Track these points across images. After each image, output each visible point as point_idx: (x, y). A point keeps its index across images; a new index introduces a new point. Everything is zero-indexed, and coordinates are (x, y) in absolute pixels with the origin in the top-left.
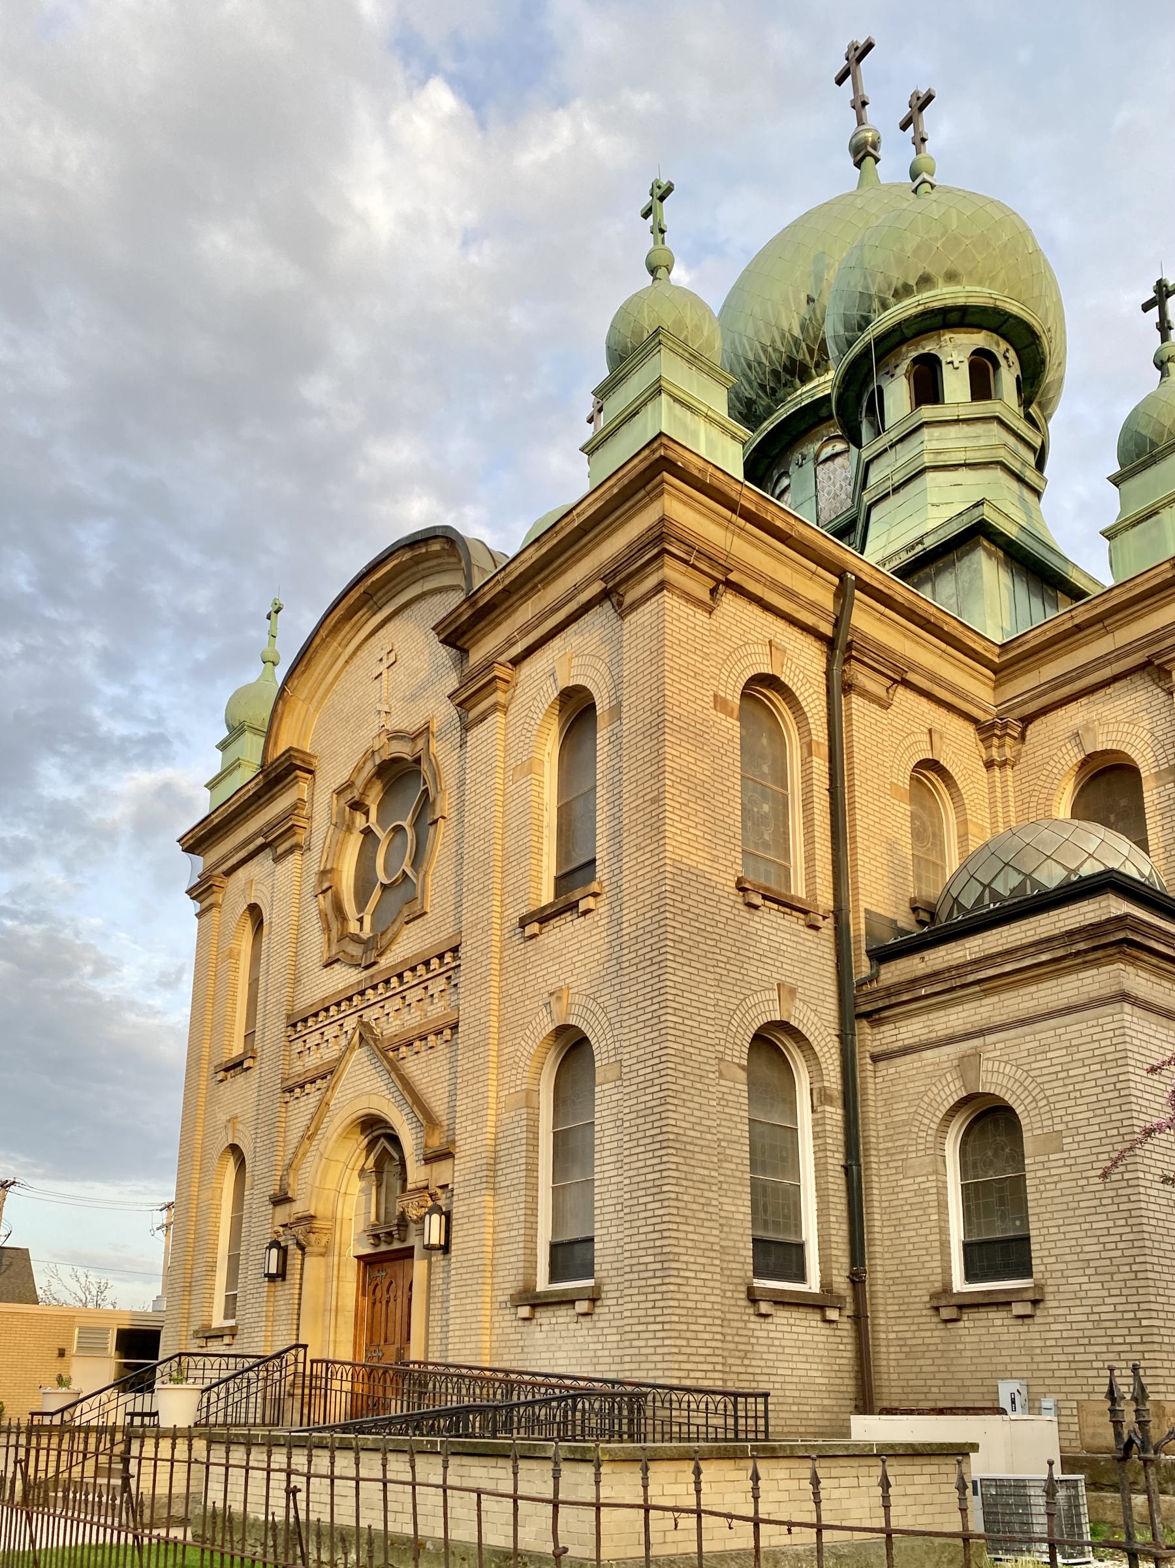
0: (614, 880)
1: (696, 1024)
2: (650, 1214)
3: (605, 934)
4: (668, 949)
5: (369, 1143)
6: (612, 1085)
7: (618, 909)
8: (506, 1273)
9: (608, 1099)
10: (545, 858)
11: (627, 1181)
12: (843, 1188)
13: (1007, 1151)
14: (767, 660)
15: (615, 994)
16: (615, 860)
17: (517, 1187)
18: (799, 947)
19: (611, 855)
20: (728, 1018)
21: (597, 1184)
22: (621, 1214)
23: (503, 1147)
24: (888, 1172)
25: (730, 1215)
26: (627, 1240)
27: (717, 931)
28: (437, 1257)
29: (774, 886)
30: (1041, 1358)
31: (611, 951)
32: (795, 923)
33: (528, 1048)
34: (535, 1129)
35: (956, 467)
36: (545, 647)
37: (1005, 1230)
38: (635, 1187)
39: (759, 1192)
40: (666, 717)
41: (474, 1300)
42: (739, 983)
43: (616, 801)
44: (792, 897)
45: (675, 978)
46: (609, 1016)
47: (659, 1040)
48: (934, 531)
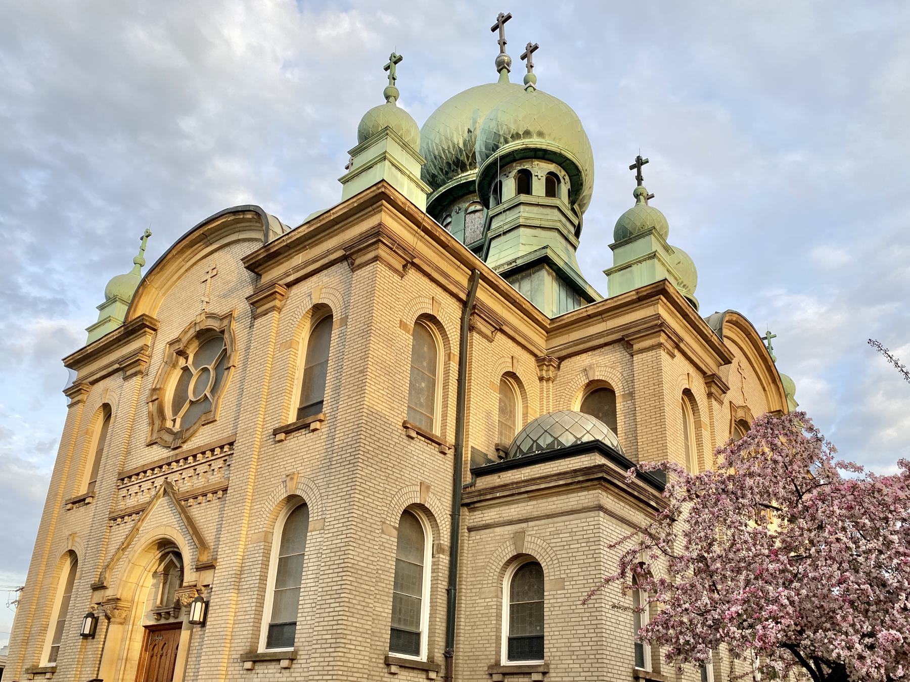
0: (333, 413)
1: (371, 501)
3: (324, 444)
4: (360, 456)
5: (162, 556)
6: (318, 532)
7: (333, 430)
9: (314, 541)
10: (293, 397)
11: (320, 590)
13: (536, 587)
14: (430, 306)
15: (325, 479)
17: (253, 589)
18: (434, 463)
20: (390, 499)
21: (302, 590)
23: (247, 564)
25: (379, 614)
27: (389, 449)
29: (423, 428)
32: (433, 449)
33: (269, 506)
34: (268, 556)
36: (307, 280)
37: (530, 632)
38: (325, 593)
43: (339, 369)
44: (433, 435)
45: (362, 473)
46: (321, 491)
47: (349, 508)
48: (522, 257)
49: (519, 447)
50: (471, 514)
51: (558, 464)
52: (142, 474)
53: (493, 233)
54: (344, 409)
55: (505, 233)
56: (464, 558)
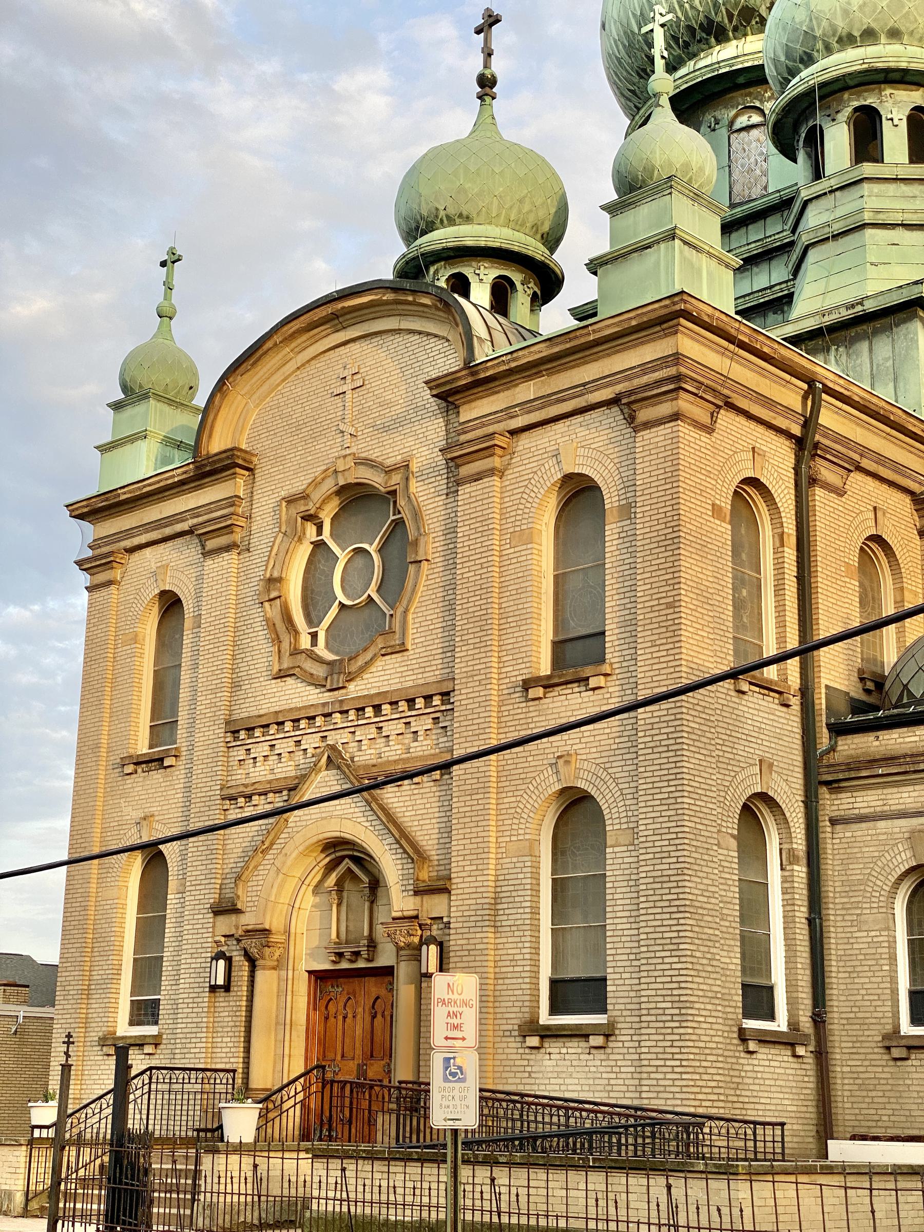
0: (625, 664)
19: (622, 641)
24: (843, 924)
31: (622, 728)
32: (770, 703)
35: (894, 226)
42: (731, 762)
46: (621, 786)
50: (834, 796)
54: (647, 662)
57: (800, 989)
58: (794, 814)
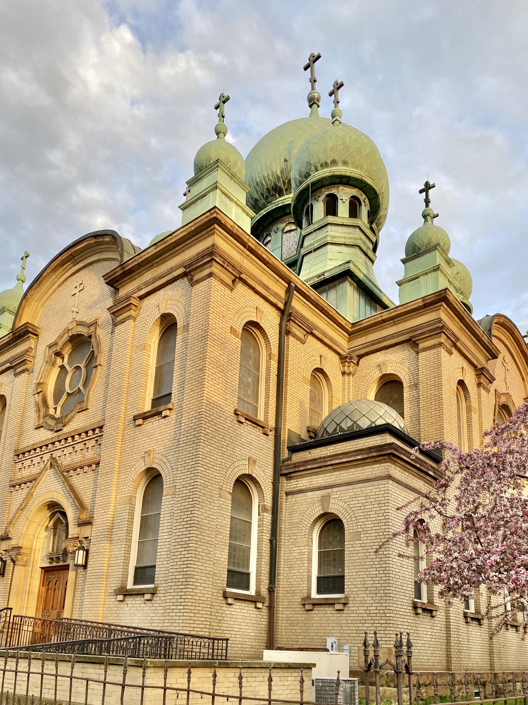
0: (179, 403)
1: (211, 472)
2: (183, 556)
3: (173, 428)
4: (201, 437)
7: (180, 417)
8: (113, 579)
11: (173, 541)
12: (269, 549)
13: (338, 538)
14: (255, 315)
15: (175, 456)
16: (181, 394)
18: (259, 442)
19: (179, 392)
20: (226, 471)
21: (159, 541)
22: (169, 556)
23: (116, 521)
24: (288, 544)
25: (219, 559)
26: (171, 567)
27: (224, 431)
28: (81, 570)
29: (250, 414)
30: (345, 628)
31: (175, 435)
32: (258, 431)
34: (132, 514)
38: (177, 544)
39: (232, 548)
40: (209, 333)
41: (97, 591)
42: (232, 455)
44: (258, 420)
46: (172, 465)
47: (194, 478)
48: (329, 270)
49: (325, 429)
50: (288, 482)
51: (357, 443)
52: (33, 451)
53: (305, 250)
55: (315, 250)
56: (283, 515)
57: (263, 575)
58: (266, 488)
